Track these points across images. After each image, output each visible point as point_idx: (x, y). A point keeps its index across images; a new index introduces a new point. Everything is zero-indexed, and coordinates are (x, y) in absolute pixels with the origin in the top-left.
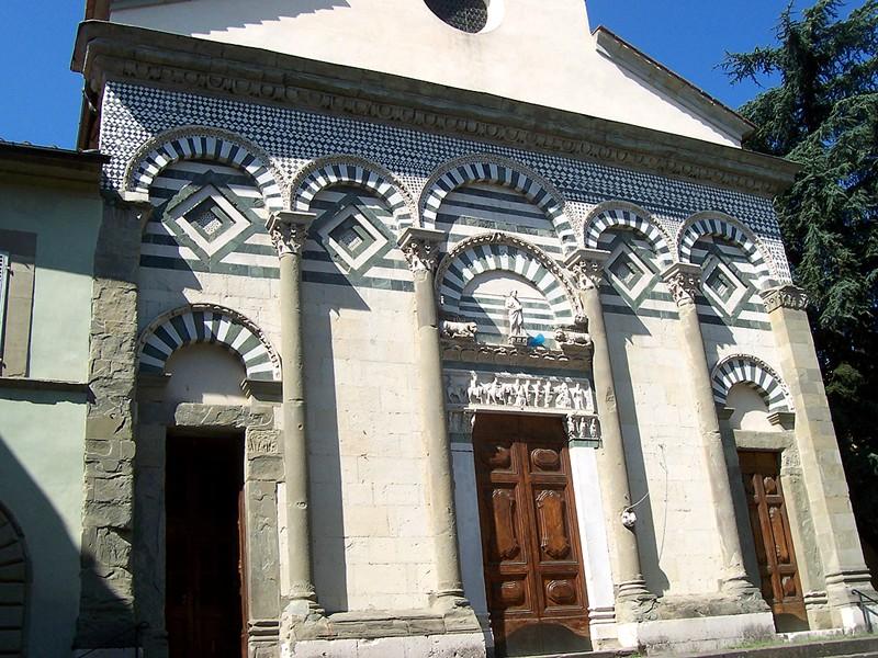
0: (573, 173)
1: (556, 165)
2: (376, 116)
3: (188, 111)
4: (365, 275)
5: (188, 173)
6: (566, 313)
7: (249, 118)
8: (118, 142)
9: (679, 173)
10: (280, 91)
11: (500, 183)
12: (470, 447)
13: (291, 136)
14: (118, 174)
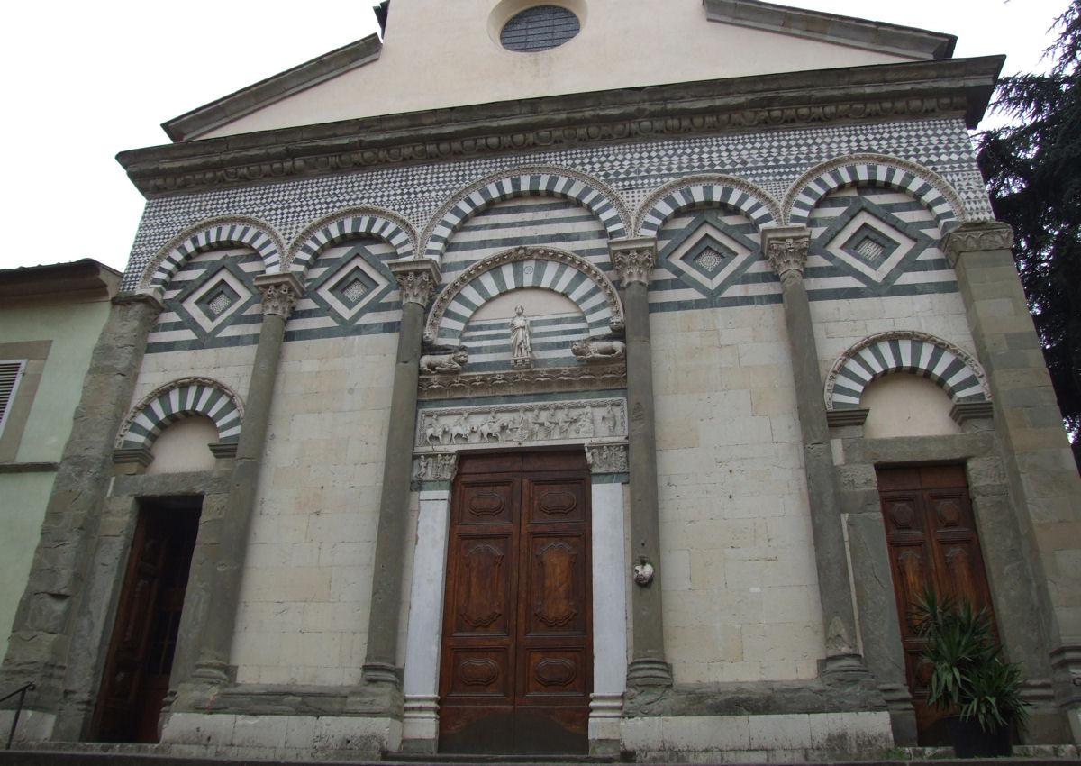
2: (386, 161)
4: (358, 323)
5: (205, 263)
9: (793, 121)
10: (288, 165)
12: (445, 494)
14: (137, 277)
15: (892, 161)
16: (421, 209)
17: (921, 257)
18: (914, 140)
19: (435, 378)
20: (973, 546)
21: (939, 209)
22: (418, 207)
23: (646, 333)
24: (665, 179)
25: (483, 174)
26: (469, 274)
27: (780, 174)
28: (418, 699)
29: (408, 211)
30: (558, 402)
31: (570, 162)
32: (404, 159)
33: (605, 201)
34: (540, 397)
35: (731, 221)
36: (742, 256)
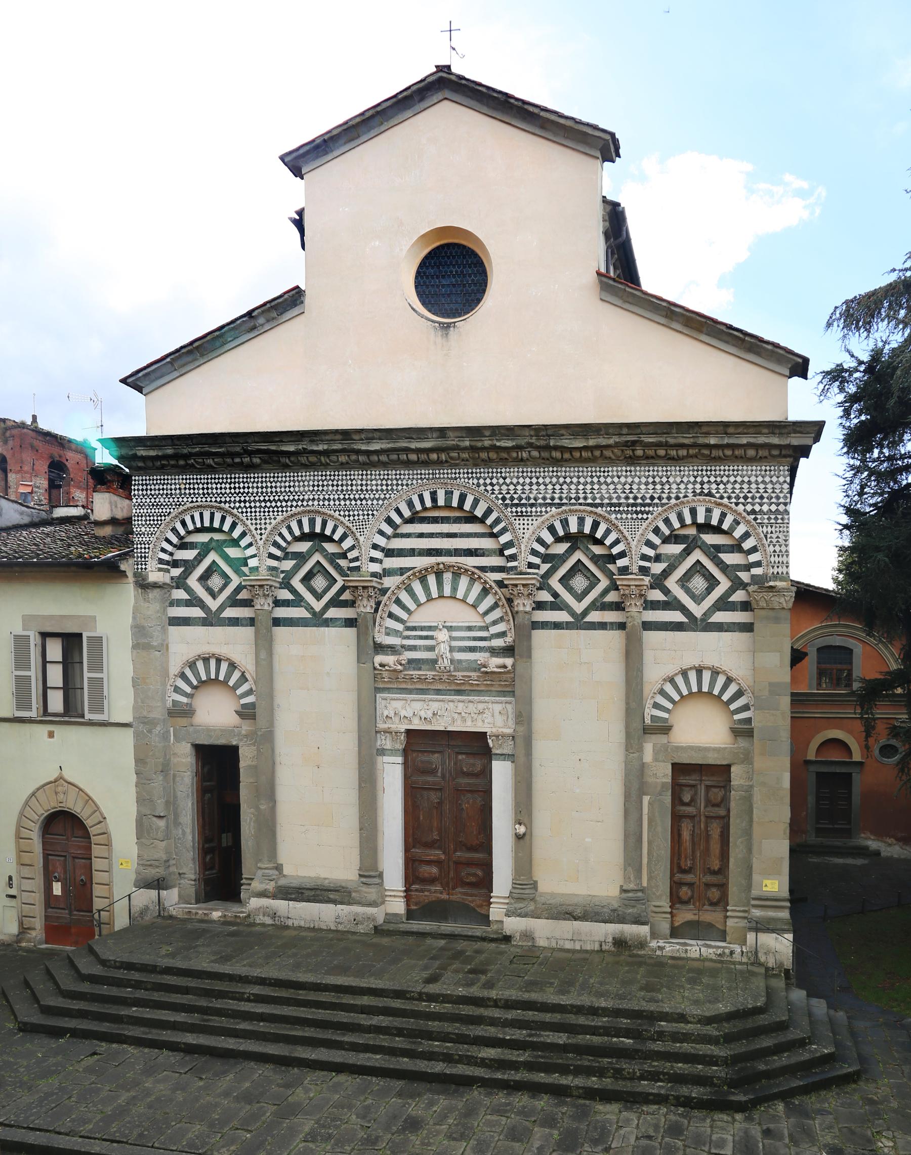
0: (523, 485)
1: (505, 478)
3: (187, 491)
4: (325, 616)
6: (503, 634)
7: (230, 488)
8: (143, 529)
9: (652, 457)
11: (448, 506)
12: (400, 760)
13: (262, 498)
14: (145, 557)
15: (726, 506)
16: (361, 517)
17: (733, 598)
18: (745, 486)
19: (385, 674)
20: (725, 821)
21: (753, 558)
22: (358, 515)
23: (529, 655)
24: (548, 509)
25: (407, 485)
26: (403, 583)
27: (637, 513)
28: (393, 891)
29: (351, 518)
30: (470, 698)
31: (475, 481)
32: (342, 464)
33: (502, 525)
34: (459, 692)
35: (597, 550)
36: (604, 583)
